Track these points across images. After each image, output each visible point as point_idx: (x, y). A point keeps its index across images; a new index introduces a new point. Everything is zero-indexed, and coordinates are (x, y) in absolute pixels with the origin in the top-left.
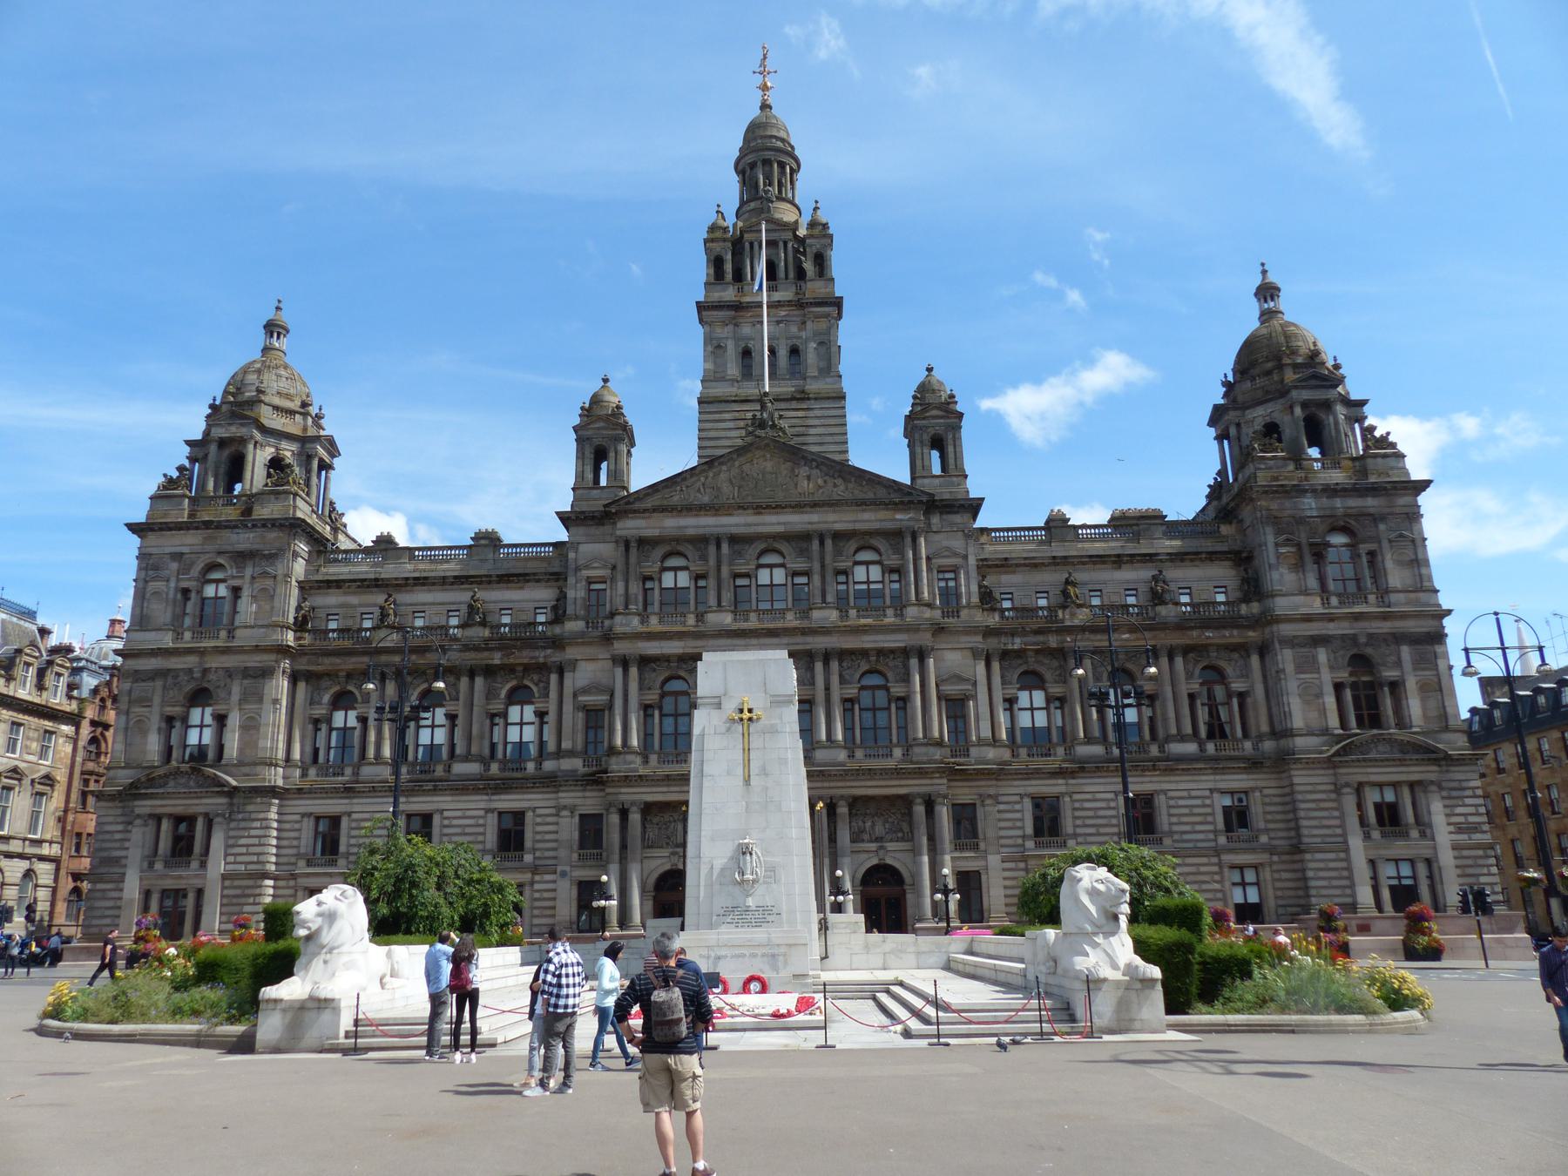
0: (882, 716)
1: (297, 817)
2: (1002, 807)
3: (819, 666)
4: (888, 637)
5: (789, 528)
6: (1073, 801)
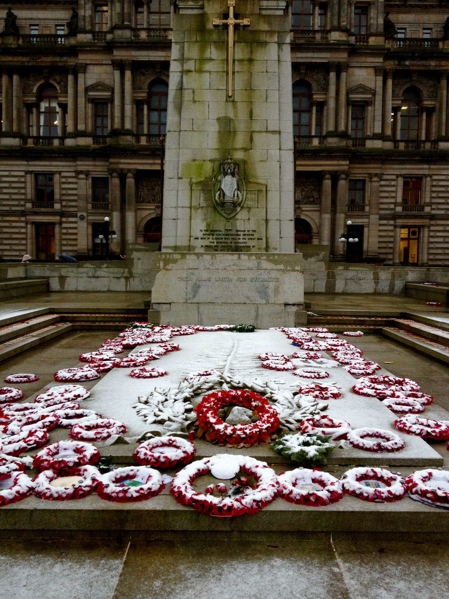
0: (305, 116)
2: (383, 183)
4: (316, 55)
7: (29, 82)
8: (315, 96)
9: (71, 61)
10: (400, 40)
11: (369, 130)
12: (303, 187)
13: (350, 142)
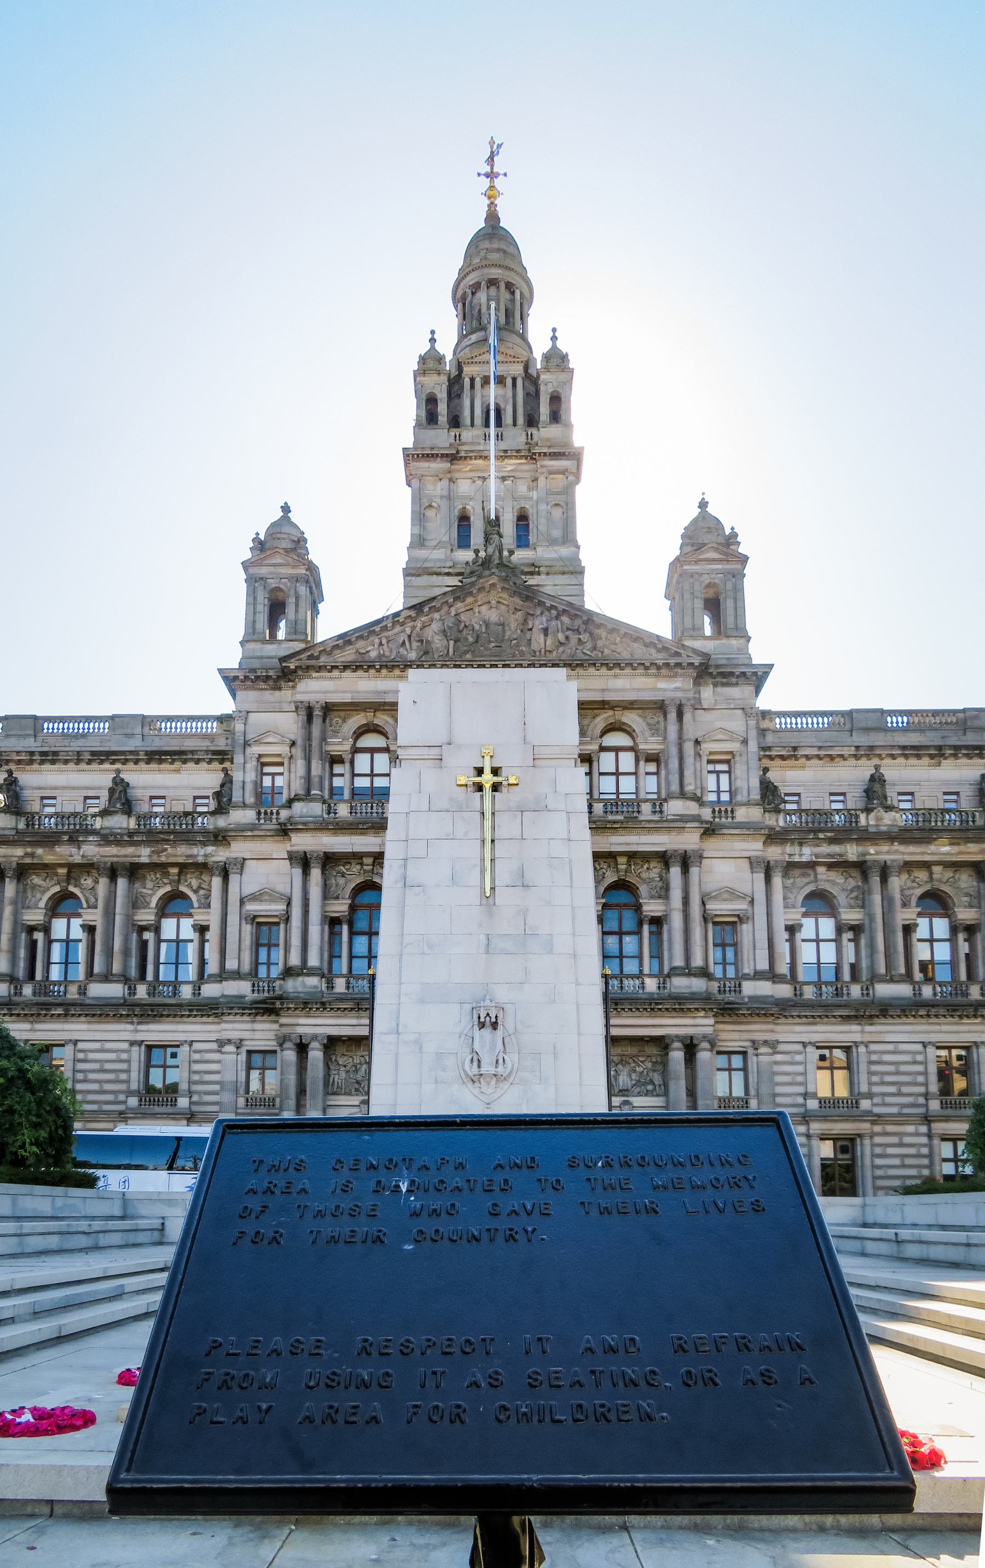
2: (779, 1057)
6: (870, 1053)
7: (145, 891)
8: (645, 908)
9: (219, 855)
10: (789, 813)
11: (746, 965)
12: (633, 1065)
13: (715, 985)
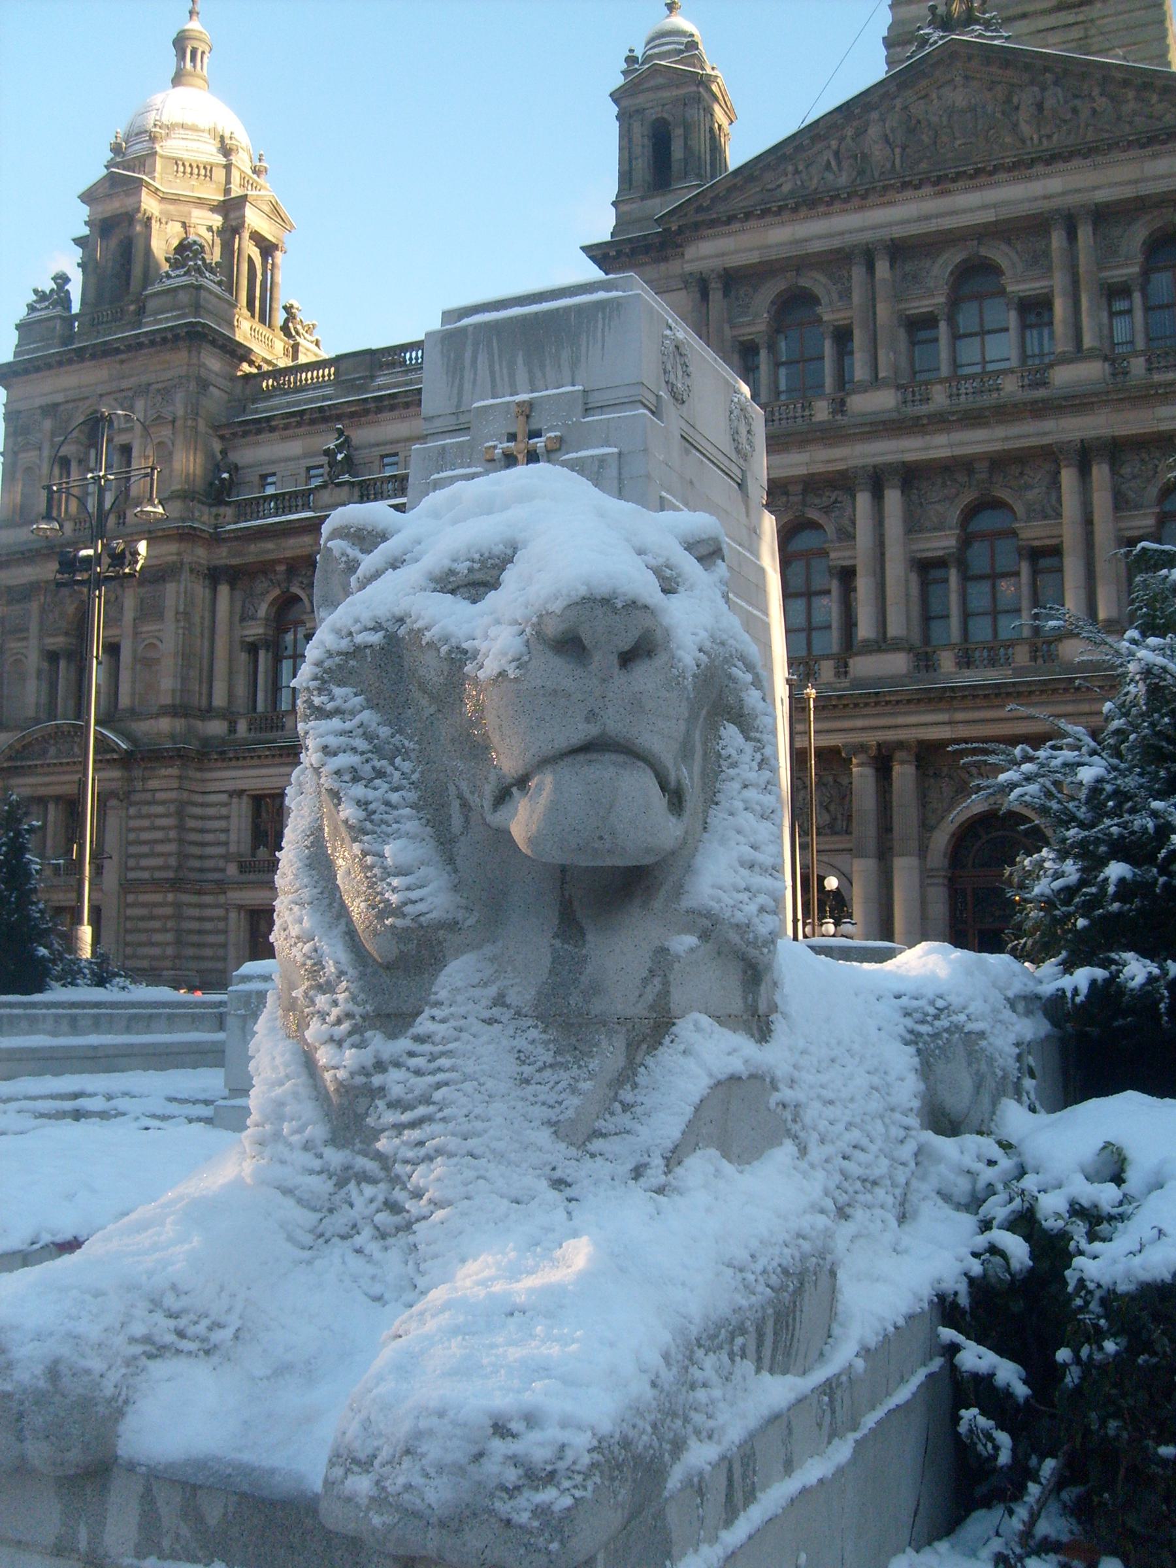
1: (224, 797)
3: (1068, 477)
5: (1005, 213)
